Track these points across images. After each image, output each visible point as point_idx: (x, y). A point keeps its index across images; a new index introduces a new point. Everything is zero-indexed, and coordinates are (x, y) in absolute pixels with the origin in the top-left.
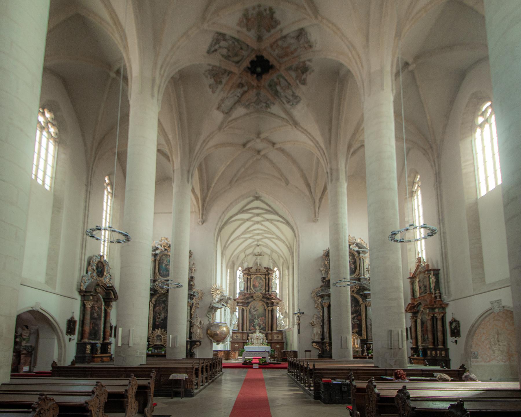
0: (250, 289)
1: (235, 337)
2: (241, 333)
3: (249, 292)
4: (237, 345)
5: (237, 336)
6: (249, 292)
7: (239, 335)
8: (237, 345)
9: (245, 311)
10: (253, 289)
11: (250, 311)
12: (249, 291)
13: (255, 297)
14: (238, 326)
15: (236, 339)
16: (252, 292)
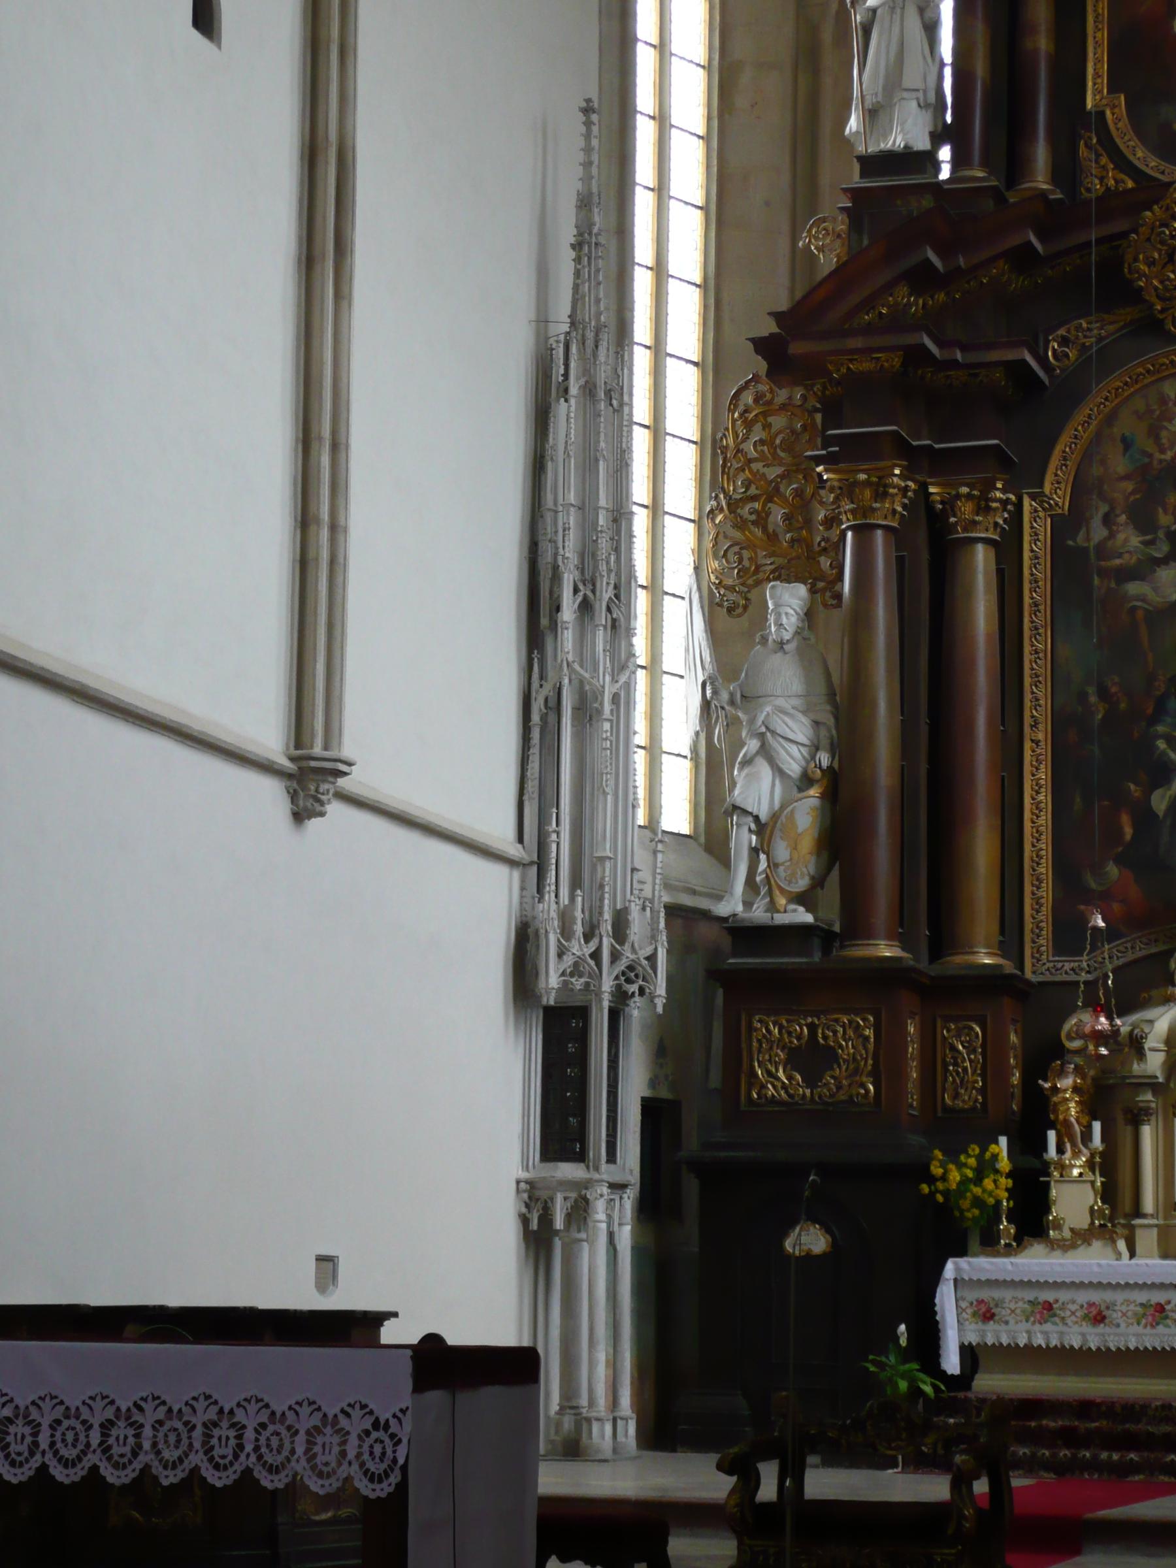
0: (1072, 119)
1: (777, 1080)
2: (885, 976)
3: (1040, 179)
4: (810, 1240)
5: (812, 1059)
6: (1040, 179)
7: (850, 1034)
8: (810, 1240)
9: (982, 559)
10: (1117, 117)
11: (1069, 562)
12: (1041, 155)
13: (1145, 271)
14: (840, 840)
15: (789, 1109)
16: (1101, 177)
